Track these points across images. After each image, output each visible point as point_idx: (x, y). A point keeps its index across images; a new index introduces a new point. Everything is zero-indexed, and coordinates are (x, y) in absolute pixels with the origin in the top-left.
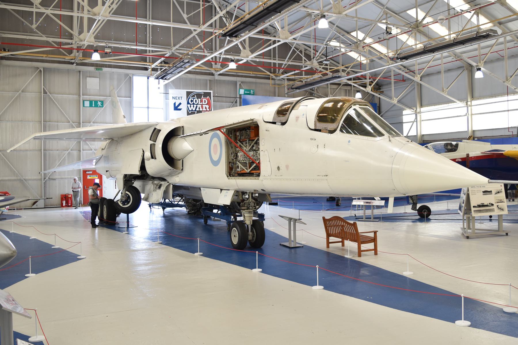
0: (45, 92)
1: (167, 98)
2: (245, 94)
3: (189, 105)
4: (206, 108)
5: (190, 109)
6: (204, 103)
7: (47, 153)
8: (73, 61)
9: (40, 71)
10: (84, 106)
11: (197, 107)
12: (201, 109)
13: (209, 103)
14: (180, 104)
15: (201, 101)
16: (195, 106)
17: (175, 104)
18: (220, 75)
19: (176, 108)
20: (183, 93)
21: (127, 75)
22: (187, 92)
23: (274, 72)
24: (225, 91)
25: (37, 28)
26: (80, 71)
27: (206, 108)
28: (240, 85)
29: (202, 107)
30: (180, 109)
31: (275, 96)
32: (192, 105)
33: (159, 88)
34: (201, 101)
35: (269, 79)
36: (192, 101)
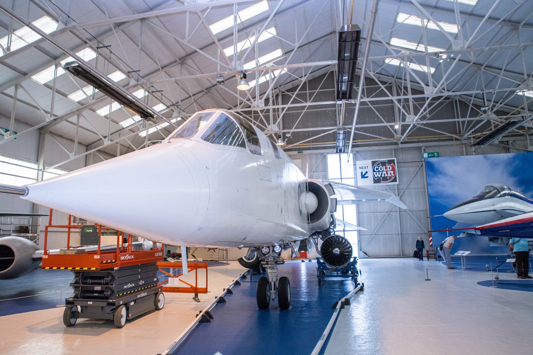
1: (355, 169)
2: (429, 157)
3: (375, 173)
4: (391, 174)
5: (376, 176)
12: (386, 175)
13: (393, 169)
14: (367, 172)
15: (386, 168)
16: (381, 173)
18: (402, 143)
19: (363, 176)
20: (369, 162)
21: (322, 154)
22: (372, 162)
23: (460, 133)
24: (409, 156)
27: (391, 174)
28: (424, 149)
29: (387, 173)
30: (367, 177)
31: (463, 155)
32: (378, 173)
33: (348, 161)
34: (386, 168)
35: (452, 140)
36: (377, 169)
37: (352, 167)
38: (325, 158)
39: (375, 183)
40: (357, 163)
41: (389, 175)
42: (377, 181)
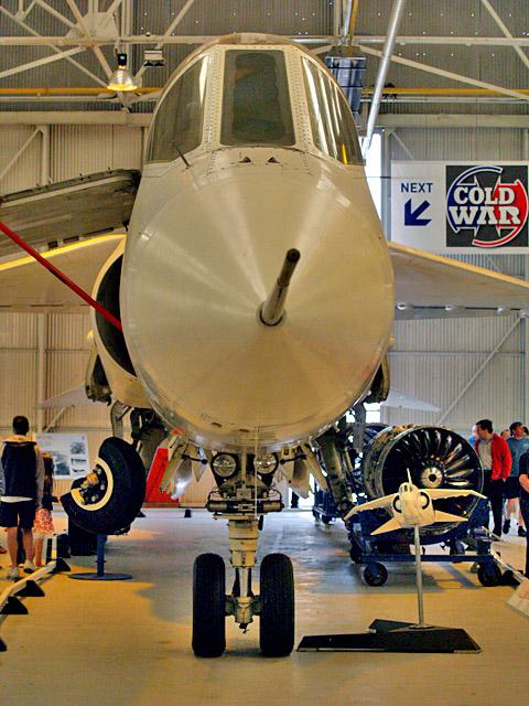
3: (453, 209)
4: (509, 216)
5: (458, 221)
6: (502, 201)
7: (56, 356)
8: (115, 100)
11: (479, 213)
12: (493, 221)
14: (425, 205)
15: (495, 195)
16: (474, 210)
19: (412, 218)
20: (436, 171)
25: (26, 20)
26: (143, 128)
27: (509, 216)
30: (424, 222)
32: (464, 209)
34: (495, 195)
36: (463, 196)
39: (451, 243)
40: (397, 168)
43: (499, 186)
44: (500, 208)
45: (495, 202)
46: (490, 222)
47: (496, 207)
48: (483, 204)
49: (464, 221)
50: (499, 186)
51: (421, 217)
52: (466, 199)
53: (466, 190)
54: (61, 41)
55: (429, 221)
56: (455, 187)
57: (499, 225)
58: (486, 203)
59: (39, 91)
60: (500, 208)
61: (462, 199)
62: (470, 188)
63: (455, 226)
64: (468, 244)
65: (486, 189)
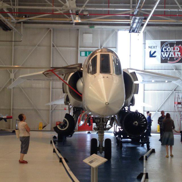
0: (53, 46)
3: (163, 53)
4: (178, 55)
5: (164, 56)
6: (176, 51)
8: (72, 22)
9: (51, 30)
10: (81, 56)
11: (169, 54)
12: (173, 56)
14: (155, 52)
15: (174, 49)
16: (168, 53)
17: (150, 52)
19: (151, 56)
20: (158, 42)
21: (113, 30)
26: (78, 30)
27: (178, 55)
29: (174, 54)
32: (165, 53)
34: (174, 49)
36: (165, 49)
37: (142, 45)
38: (116, 34)
41: (176, 56)
42: (164, 60)
43: (175, 47)
44: (175, 53)
45: (174, 51)
46: (173, 56)
47: (174, 52)
48: (171, 52)
49: (165, 56)
50: (175, 47)
51: (153, 55)
52: (166, 50)
53: (166, 48)
54: (61, 8)
55: (156, 56)
56: (163, 47)
57: (175, 57)
58: (171, 51)
59: (51, 19)
60: (175, 53)
61: (165, 50)
62: (167, 47)
63: (163, 58)
64: (167, 63)
65: (171, 47)
